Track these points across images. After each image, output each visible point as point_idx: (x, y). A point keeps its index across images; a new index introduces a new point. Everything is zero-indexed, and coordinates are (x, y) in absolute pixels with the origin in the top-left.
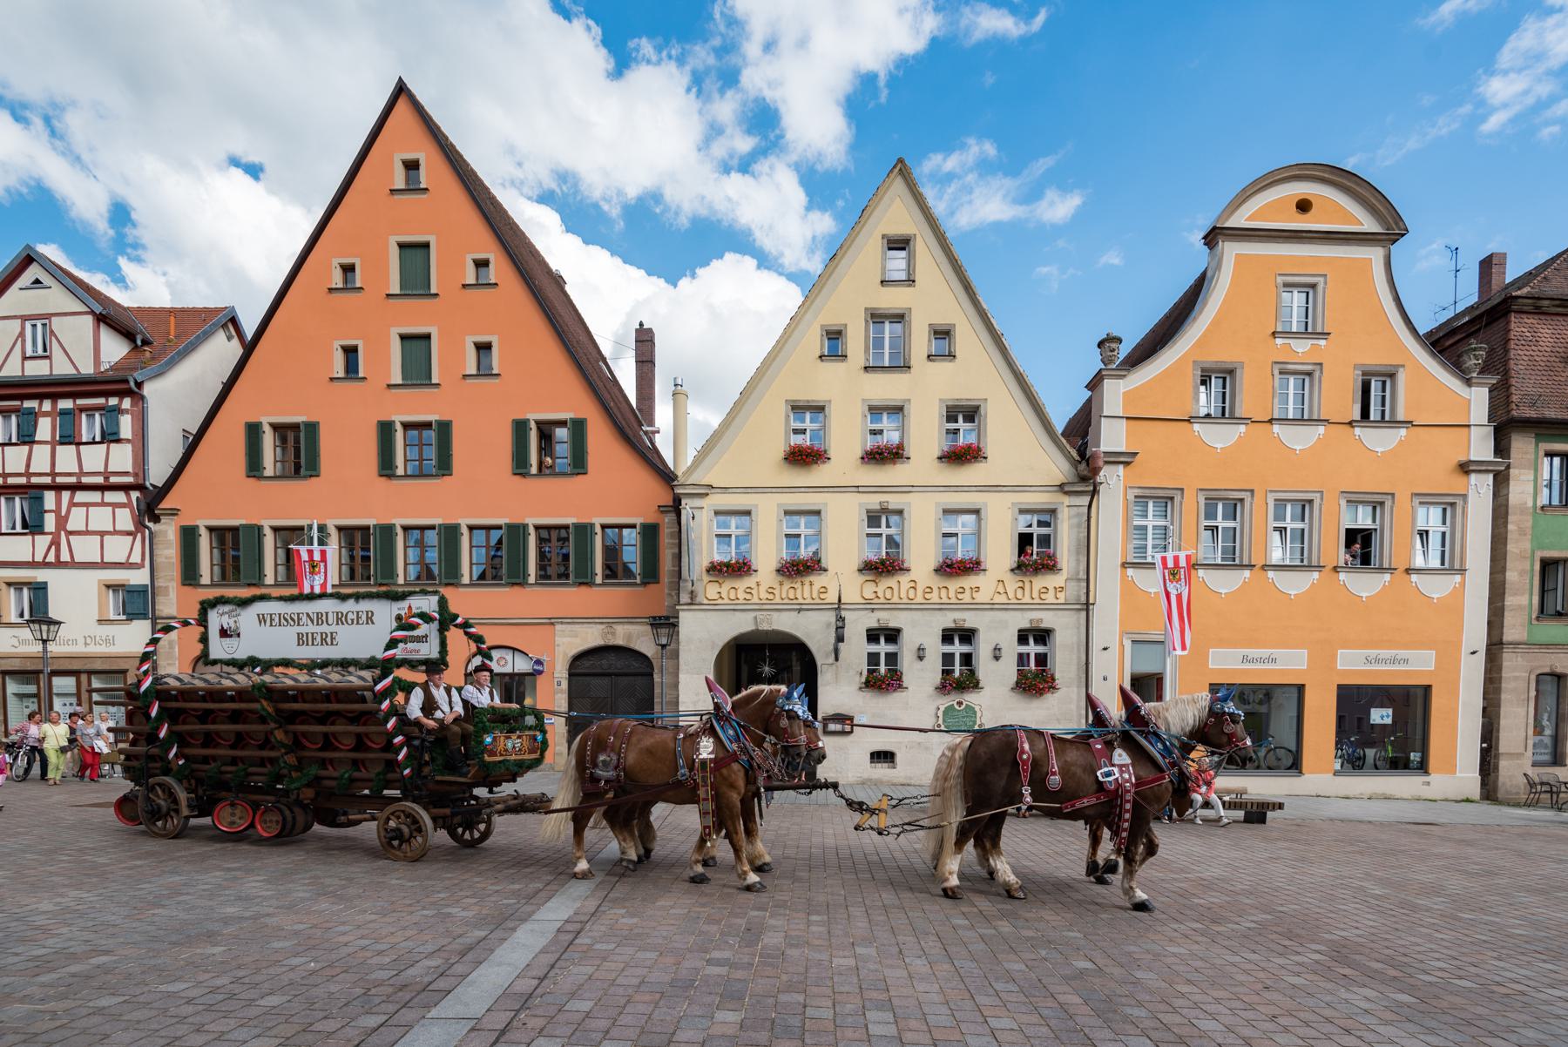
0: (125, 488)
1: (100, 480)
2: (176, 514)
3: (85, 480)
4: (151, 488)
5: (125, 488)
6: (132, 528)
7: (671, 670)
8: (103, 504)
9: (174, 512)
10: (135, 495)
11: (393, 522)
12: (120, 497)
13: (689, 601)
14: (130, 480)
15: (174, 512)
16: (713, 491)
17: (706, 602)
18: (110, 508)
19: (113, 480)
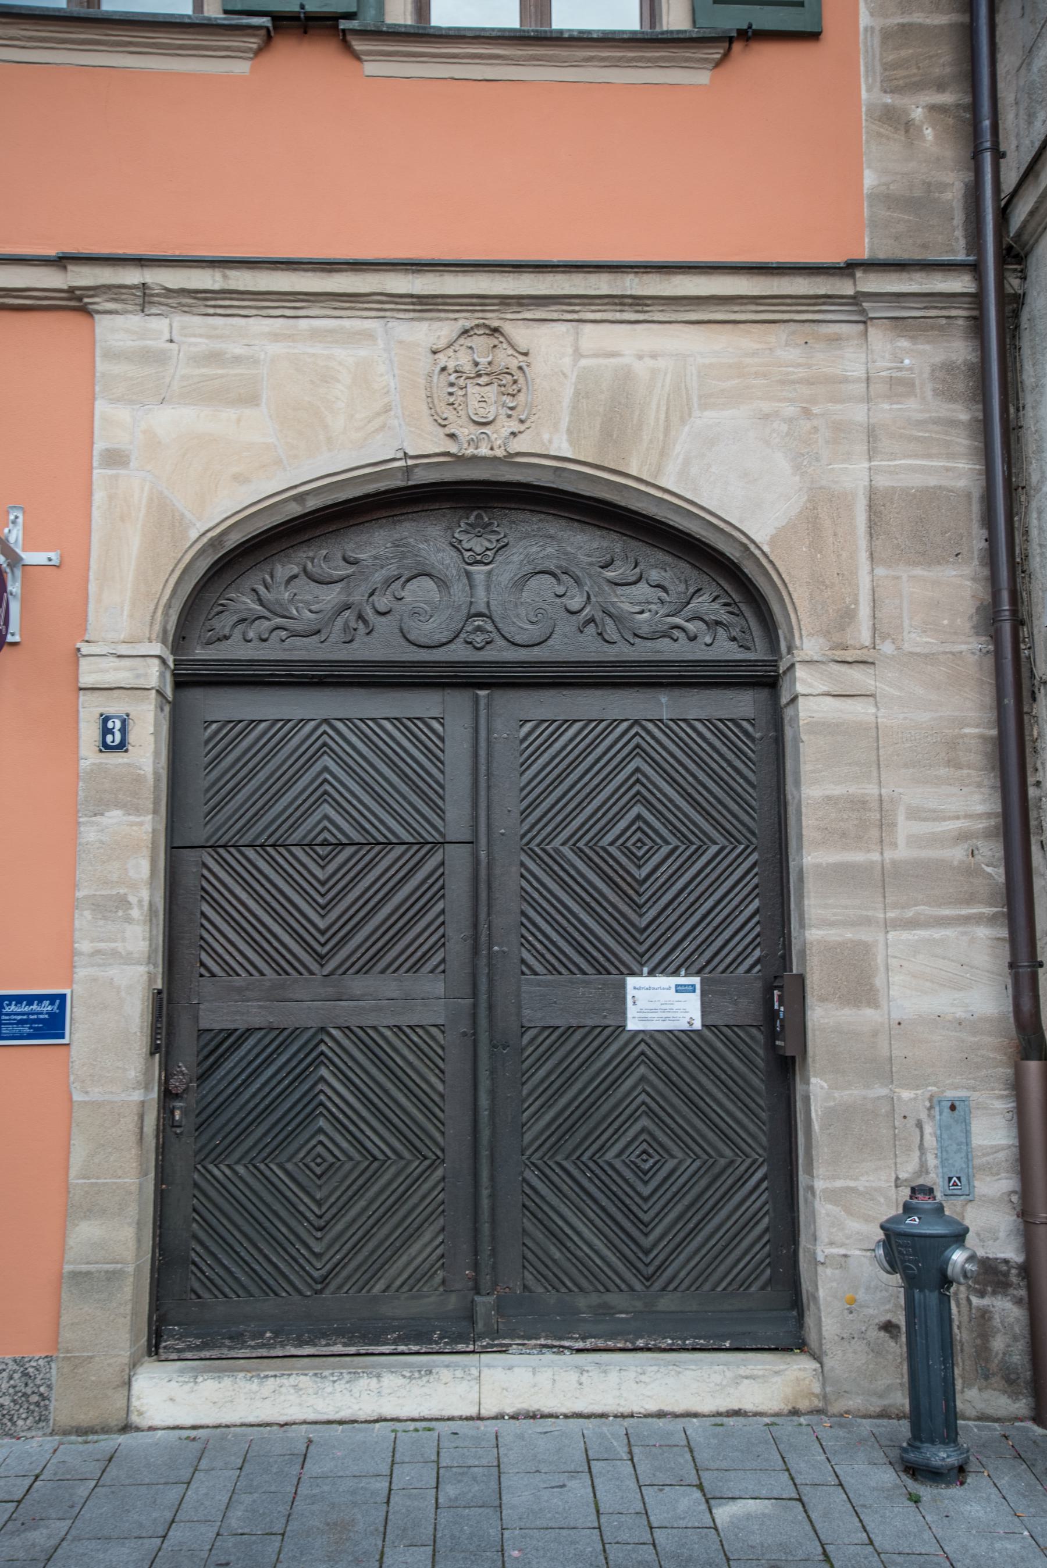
7: (916, 640)
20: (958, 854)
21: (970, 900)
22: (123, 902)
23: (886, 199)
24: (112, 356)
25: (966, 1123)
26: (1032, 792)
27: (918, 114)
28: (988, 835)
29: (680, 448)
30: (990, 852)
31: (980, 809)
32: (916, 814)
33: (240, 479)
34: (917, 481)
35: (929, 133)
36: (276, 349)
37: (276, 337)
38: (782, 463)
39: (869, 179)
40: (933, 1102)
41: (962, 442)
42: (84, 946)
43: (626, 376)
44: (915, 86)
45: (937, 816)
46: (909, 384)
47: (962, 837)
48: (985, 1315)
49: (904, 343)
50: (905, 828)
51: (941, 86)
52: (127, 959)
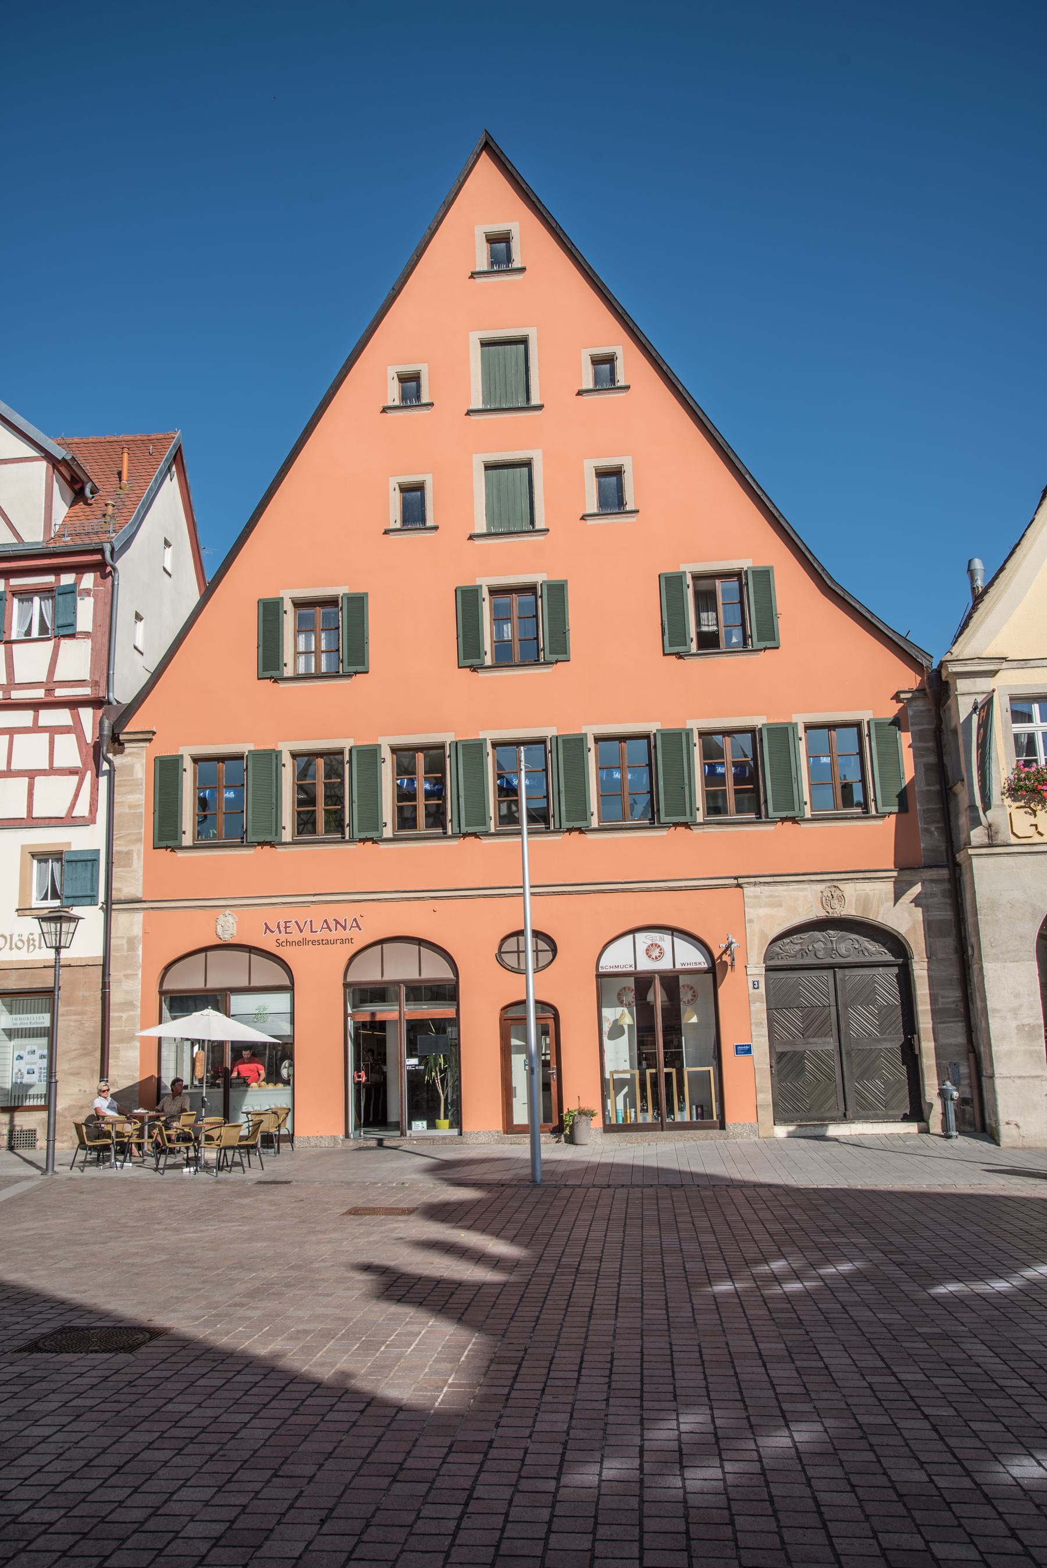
0: (73, 704)
1: (39, 694)
2: (150, 740)
3: (16, 695)
4: (115, 703)
5: (73, 704)
6: (76, 762)
8: (36, 729)
9: (147, 736)
10: (87, 715)
11: (482, 735)
12: (62, 717)
13: (986, 840)
14: (85, 691)
15: (147, 736)
16: (1005, 665)
17: (1014, 840)
18: (46, 735)
19: (60, 693)
20: (953, 1006)
21: (957, 1017)
22: (761, 1023)
23: (925, 850)
24: (748, 897)
25: (958, 1067)
26: (969, 991)
27: (933, 829)
28: (960, 1001)
29: (881, 912)
30: (961, 1005)
31: (958, 995)
32: (943, 997)
33: (779, 924)
34: (939, 917)
35: (936, 833)
36: (785, 893)
37: (785, 891)
38: (906, 915)
39: (922, 845)
40: (950, 1063)
41: (948, 908)
42: (754, 1033)
43: (867, 895)
44: (932, 823)
45: (948, 997)
46: (935, 894)
47: (954, 1002)
48: (964, 1110)
49: (933, 885)
50: (940, 1000)
51: (938, 823)
52: (764, 1036)
